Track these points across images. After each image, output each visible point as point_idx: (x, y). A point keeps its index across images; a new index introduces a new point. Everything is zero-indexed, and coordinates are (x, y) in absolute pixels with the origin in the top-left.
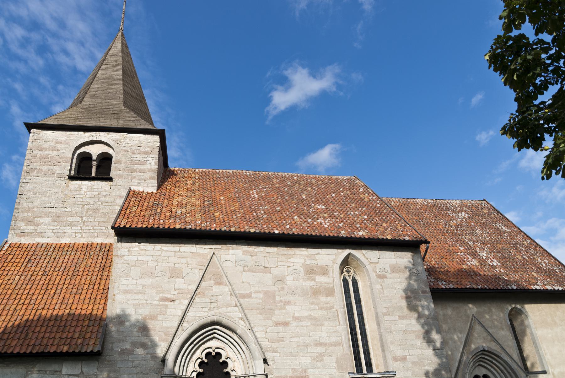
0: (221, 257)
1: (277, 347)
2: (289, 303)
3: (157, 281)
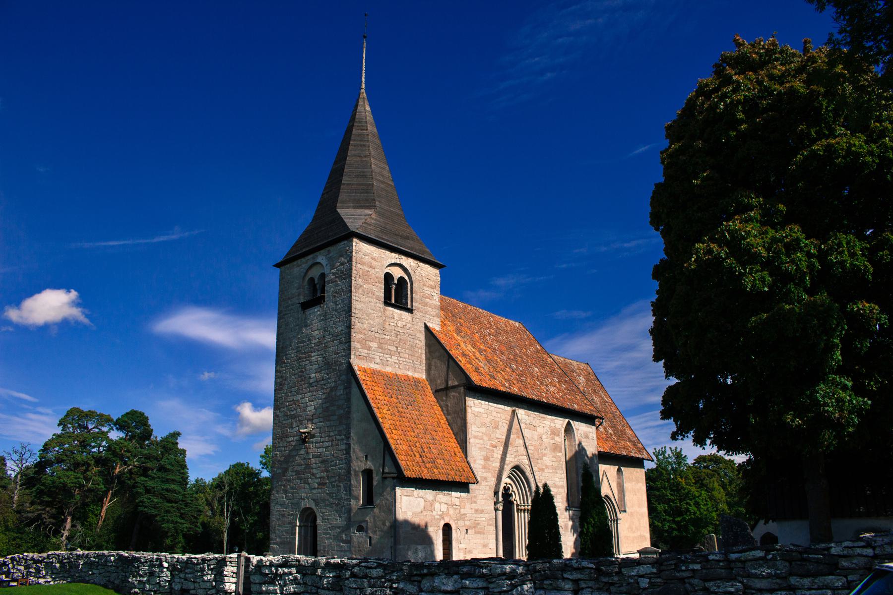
2: (544, 455)
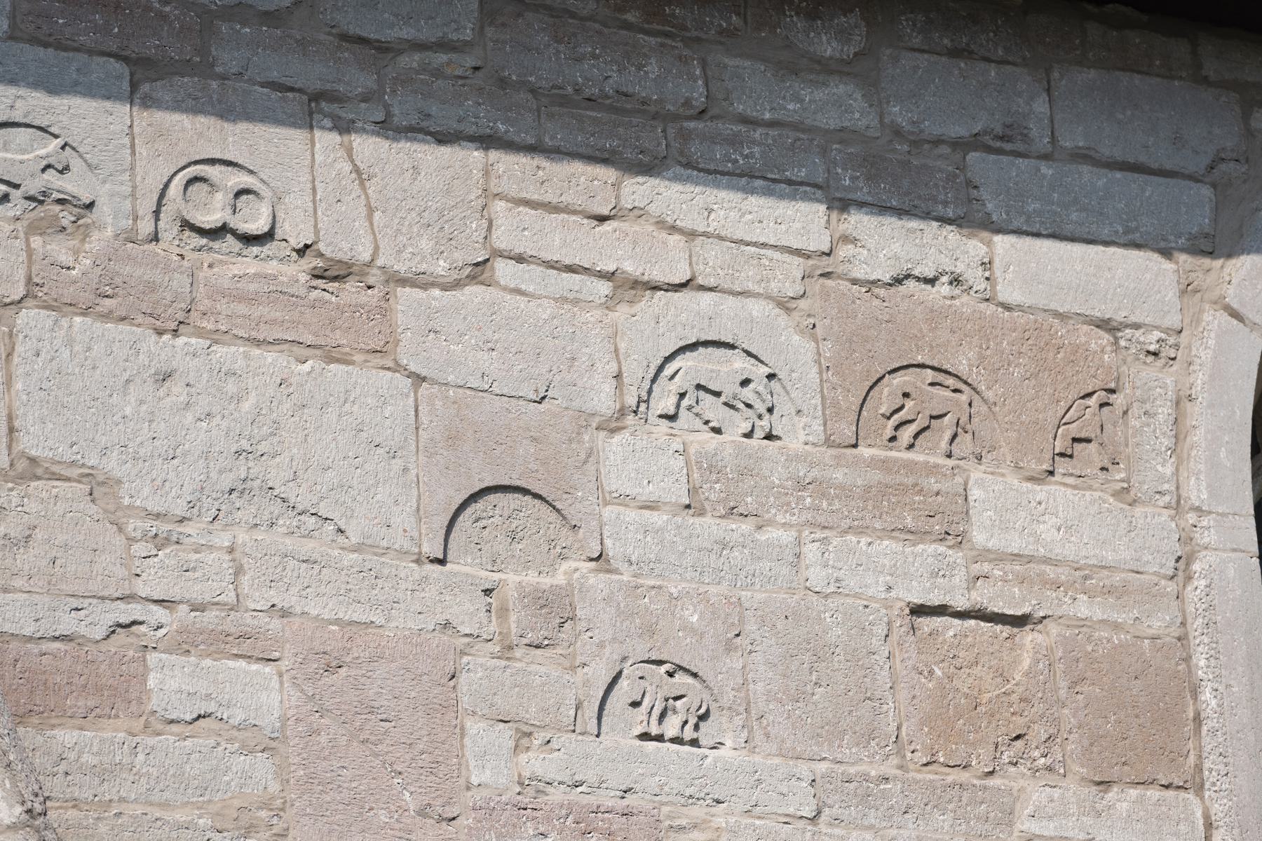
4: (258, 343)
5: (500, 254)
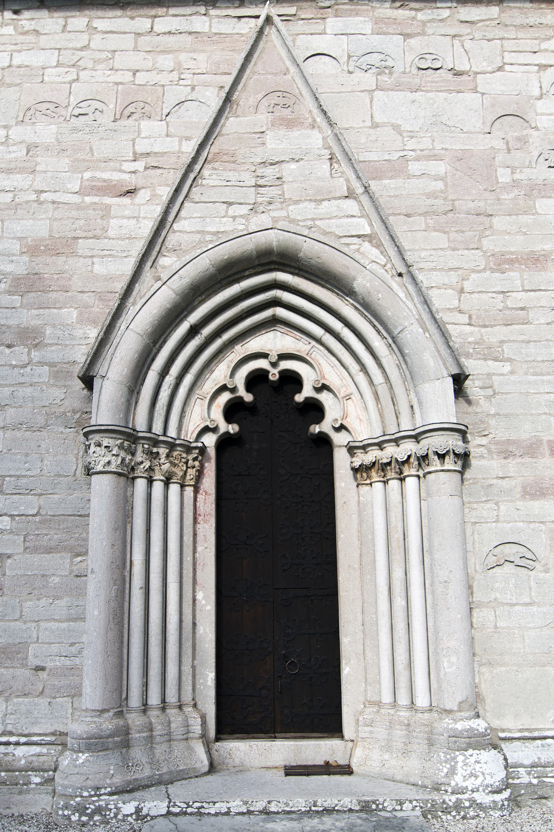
0: (298, 43)
1: (502, 342)
3: (75, 130)
4: (439, 91)
5: (506, 64)
